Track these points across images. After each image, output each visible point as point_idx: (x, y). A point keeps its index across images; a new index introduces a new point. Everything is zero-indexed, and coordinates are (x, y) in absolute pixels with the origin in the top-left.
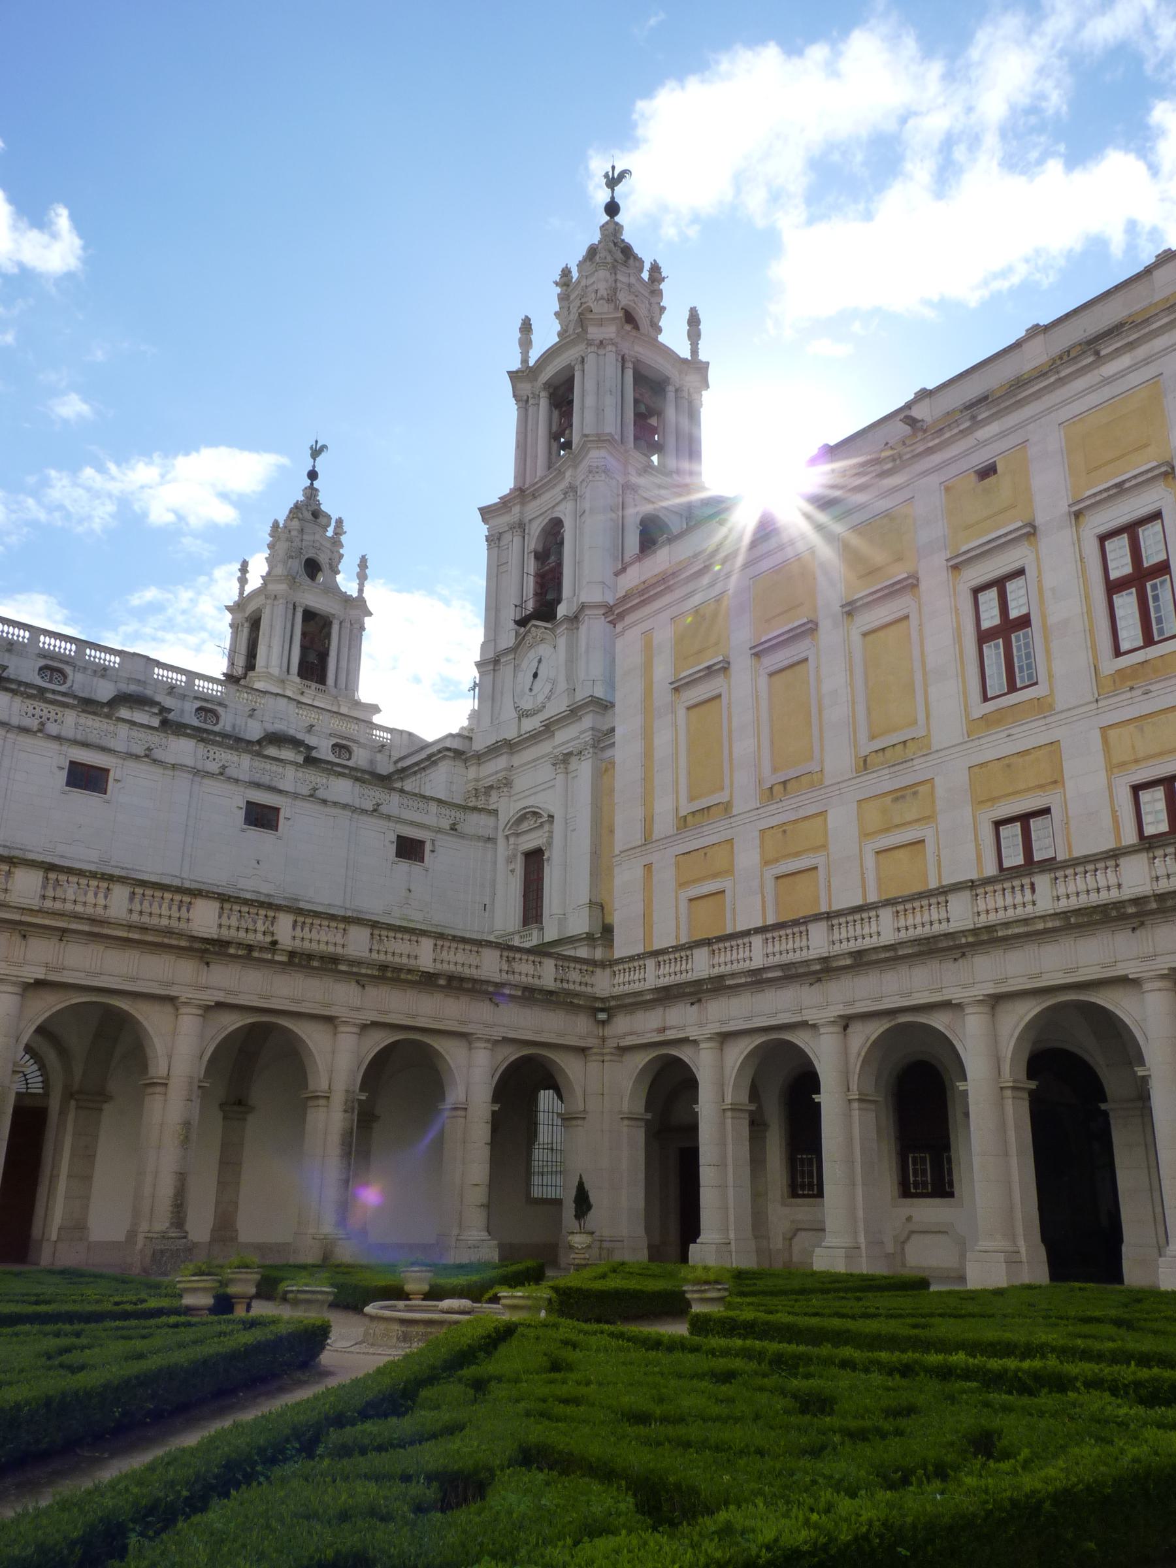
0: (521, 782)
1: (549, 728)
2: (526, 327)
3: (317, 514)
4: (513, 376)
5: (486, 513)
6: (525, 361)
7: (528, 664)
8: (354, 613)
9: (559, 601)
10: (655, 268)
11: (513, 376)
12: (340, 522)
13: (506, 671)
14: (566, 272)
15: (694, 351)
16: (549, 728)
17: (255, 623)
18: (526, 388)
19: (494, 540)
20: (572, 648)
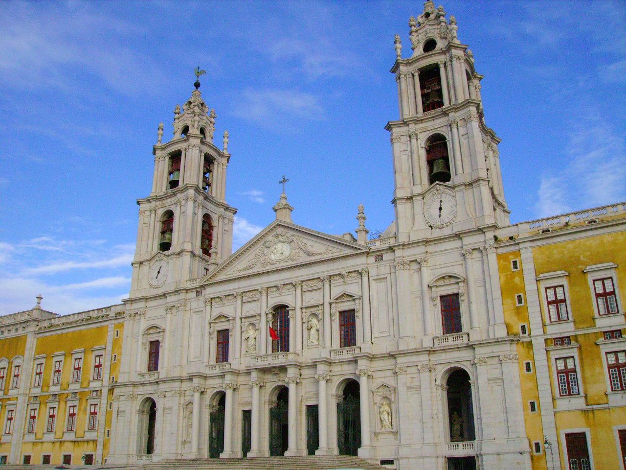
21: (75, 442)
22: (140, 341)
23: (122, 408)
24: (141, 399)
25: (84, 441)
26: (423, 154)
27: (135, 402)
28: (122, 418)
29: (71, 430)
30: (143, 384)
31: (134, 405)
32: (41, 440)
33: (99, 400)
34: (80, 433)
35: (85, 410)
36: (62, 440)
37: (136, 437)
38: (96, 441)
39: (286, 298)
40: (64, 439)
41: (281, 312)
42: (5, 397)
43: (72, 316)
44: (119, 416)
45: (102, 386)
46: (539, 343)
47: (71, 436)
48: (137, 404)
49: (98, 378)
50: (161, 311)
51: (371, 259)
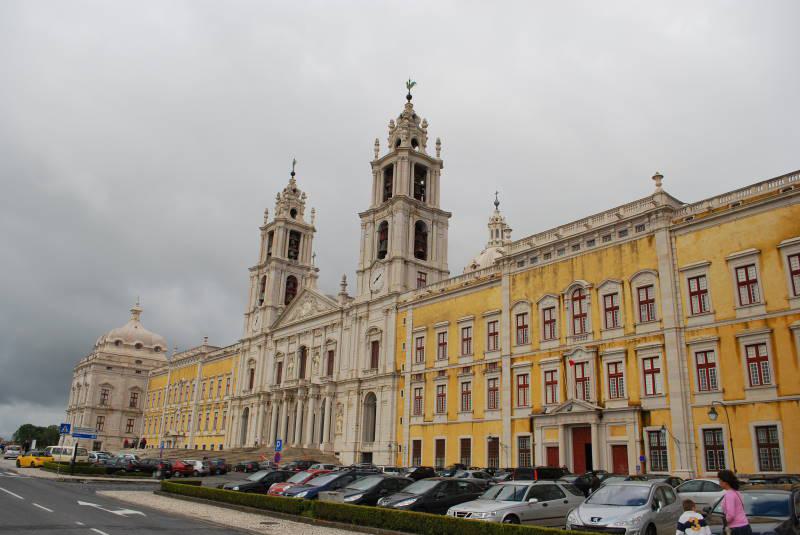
0: (373, 316)
1: (381, 299)
2: (377, 144)
3: (295, 191)
4: (373, 164)
5: (361, 215)
6: (376, 157)
7: (376, 273)
8: (310, 233)
9: (386, 252)
10: (425, 122)
11: (373, 164)
12: (304, 194)
13: (368, 272)
14: (392, 122)
15: (438, 155)
16: (381, 299)
17: (271, 234)
18: (376, 168)
19: (364, 226)
20: (389, 271)
22: (246, 369)
26: (377, 235)
39: (308, 342)
41: (303, 350)
46: (408, 377)
49: (227, 395)
50: (257, 349)
51: (344, 315)
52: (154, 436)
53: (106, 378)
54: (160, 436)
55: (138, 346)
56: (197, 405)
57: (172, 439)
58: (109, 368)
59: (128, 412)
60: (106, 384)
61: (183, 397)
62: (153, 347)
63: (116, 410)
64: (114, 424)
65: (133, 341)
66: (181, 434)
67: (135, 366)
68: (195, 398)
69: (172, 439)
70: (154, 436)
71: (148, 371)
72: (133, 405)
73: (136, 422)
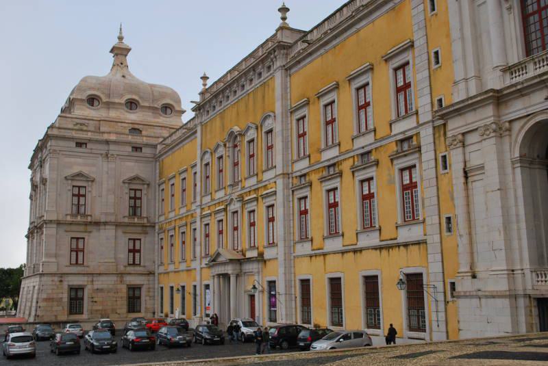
21: (380, 248)
23: (474, 161)
24: (520, 132)
25: (398, 246)
27: (506, 140)
28: (477, 186)
29: (371, 226)
30: (521, 92)
31: (507, 147)
32: (321, 251)
33: (417, 155)
34: (387, 234)
35: (391, 182)
36: (357, 247)
37: (523, 225)
38: (425, 242)
40: (361, 244)
42: (260, 185)
43: (338, 14)
44: (470, 179)
45: (419, 125)
47: (373, 239)
48: (514, 147)
52: (183, 266)
53: (77, 164)
54: (195, 265)
55: (132, 104)
56: (286, 175)
57: (229, 269)
58: (79, 145)
59: (128, 225)
60: (80, 175)
61: (243, 169)
62: (158, 105)
63: (105, 223)
64: (105, 248)
65: (122, 96)
66: (252, 254)
67: (130, 138)
68: (278, 160)
69: (229, 269)
70: (183, 266)
71: (155, 146)
72: (134, 210)
73: (146, 243)
